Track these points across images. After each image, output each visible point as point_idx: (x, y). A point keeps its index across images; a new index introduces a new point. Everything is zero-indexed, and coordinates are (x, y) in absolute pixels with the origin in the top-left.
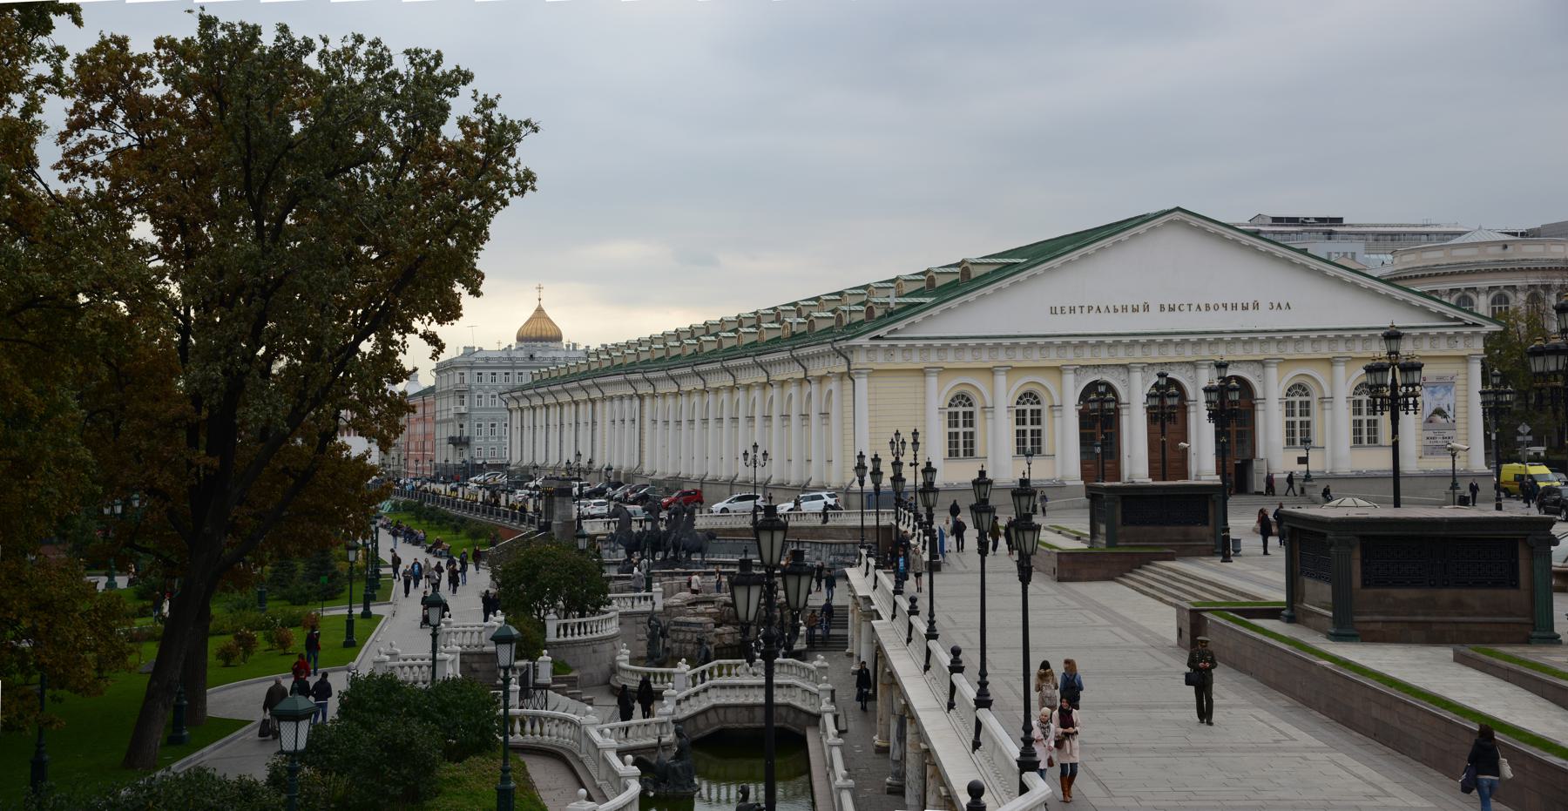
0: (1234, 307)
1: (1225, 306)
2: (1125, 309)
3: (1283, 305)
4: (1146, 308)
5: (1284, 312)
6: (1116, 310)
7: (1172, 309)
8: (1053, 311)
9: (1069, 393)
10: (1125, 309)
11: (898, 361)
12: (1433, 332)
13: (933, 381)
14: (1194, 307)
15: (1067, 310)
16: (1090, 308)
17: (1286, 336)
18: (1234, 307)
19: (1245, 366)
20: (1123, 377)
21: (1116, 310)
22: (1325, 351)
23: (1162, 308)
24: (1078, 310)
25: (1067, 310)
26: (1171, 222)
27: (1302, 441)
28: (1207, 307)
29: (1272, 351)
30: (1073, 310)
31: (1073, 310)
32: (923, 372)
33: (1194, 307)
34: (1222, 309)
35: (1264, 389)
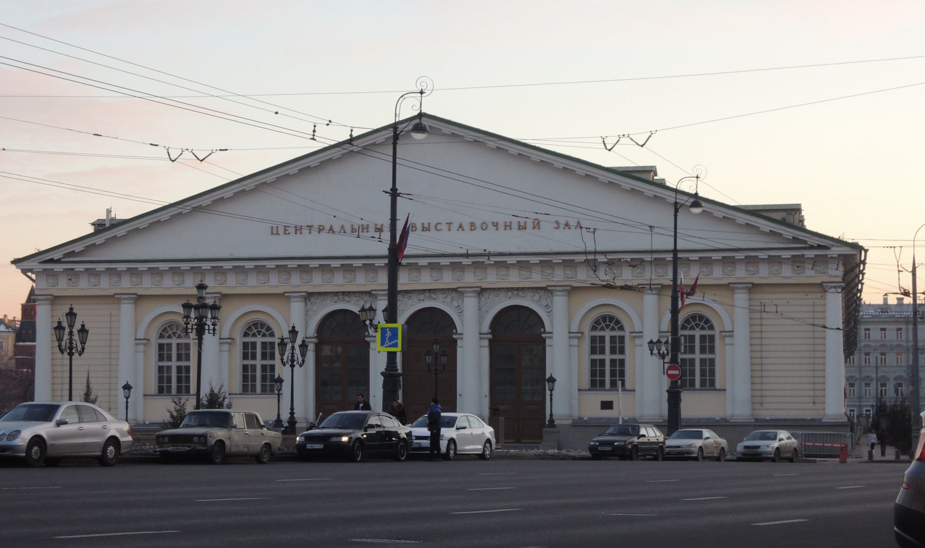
1: (496, 225)
8: (274, 232)
13: (127, 309)
14: (455, 227)
28: (472, 225)
33: (455, 227)
34: (491, 228)
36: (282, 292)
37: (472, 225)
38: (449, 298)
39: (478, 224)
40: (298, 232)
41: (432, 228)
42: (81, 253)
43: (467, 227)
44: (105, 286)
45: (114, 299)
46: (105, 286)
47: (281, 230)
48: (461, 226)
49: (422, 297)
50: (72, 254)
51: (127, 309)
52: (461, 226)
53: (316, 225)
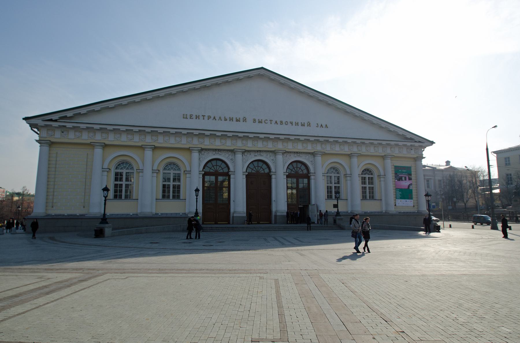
1: (292, 123)
3: (324, 126)
4: (245, 120)
6: (226, 120)
7: (260, 122)
8: (185, 117)
10: (231, 119)
11: (72, 137)
13: (98, 151)
14: (273, 122)
15: (194, 117)
16: (209, 117)
20: (231, 157)
21: (226, 120)
22: (346, 150)
23: (254, 121)
24: (201, 118)
25: (194, 117)
27: (336, 197)
28: (281, 122)
29: (319, 148)
31: (197, 117)
32: (92, 145)
33: (273, 122)
34: (290, 124)
35: (315, 168)
39: (284, 122)
41: (263, 122)
42: (71, 118)
43: (279, 122)
44: (85, 137)
45: (92, 145)
46: (85, 137)
47: (188, 117)
48: (276, 122)
49: (256, 154)
50: (65, 117)
51: (98, 151)
52: (276, 122)
53: (207, 115)
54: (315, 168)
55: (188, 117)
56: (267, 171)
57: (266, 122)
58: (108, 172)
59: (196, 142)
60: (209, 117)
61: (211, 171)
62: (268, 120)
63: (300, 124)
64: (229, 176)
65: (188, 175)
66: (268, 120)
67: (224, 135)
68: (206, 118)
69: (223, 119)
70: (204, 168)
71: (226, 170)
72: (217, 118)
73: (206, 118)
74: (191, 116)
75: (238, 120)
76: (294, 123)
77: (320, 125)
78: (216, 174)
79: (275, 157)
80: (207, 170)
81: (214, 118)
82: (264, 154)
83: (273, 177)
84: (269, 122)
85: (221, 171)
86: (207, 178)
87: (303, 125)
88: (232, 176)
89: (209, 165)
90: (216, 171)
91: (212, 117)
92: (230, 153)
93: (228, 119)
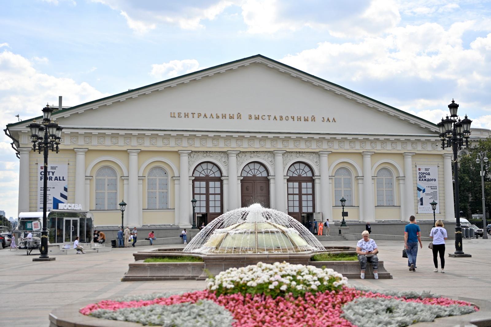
0: (299, 119)
1: (293, 118)
2: (224, 116)
3: (331, 120)
5: (332, 124)
6: (218, 117)
7: (257, 118)
9: (186, 168)
12: (423, 139)
15: (183, 115)
17: (332, 138)
18: (299, 119)
19: (307, 155)
21: (218, 117)
22: (358, 148)
24: (190, 115)
25: (183, 115)
26: (255, 63)
28: (281, 117)
30: (186, 115)
31: (186, 115)
34: (290, 119)
35: (320, 170)
36: (177, 150)
37: (281, 117)
38: (266, 157)
39: (284, 118)
40: (187, 116)
41: (260, 118)
43: (278, 118)
47: (176, 115)
48: (275, 118)
49: (252, 155)
52: (275, 118)
54: (320, 170)
55: (176, 115)
56: (264, 174)
57: (264, 118)
58: (90, 180)
59: (185, 145)
60: (199, 115)
61: (202, 175)
62: (266, 115)
63: (302, 119)
64: (222, 182)
65: (176, 182)
66: (266, 115)
67: (217, 135)
68: (196, 116)
69: (215, 116)
70: (193, 173)
71: (218, 175)
72: (208, 115)
73: (196, 116)
74: (179, 114)
75: (231, 117)
76: (296, 119)
77: (326, 119)
78: (207, 179)
79: (274, 158)
80: (197, 174)
81: (205, 115)
82: (262, 155)
83: (272, 181)
84: (267, 118)
85: (213, 175)
86: (197, 184)
87: (306, 120)
88: (225, 182)
89: (200, 169)
90: (207, 176)
91: (203, 115)
92: (222, 155)
93: (221, 117)
